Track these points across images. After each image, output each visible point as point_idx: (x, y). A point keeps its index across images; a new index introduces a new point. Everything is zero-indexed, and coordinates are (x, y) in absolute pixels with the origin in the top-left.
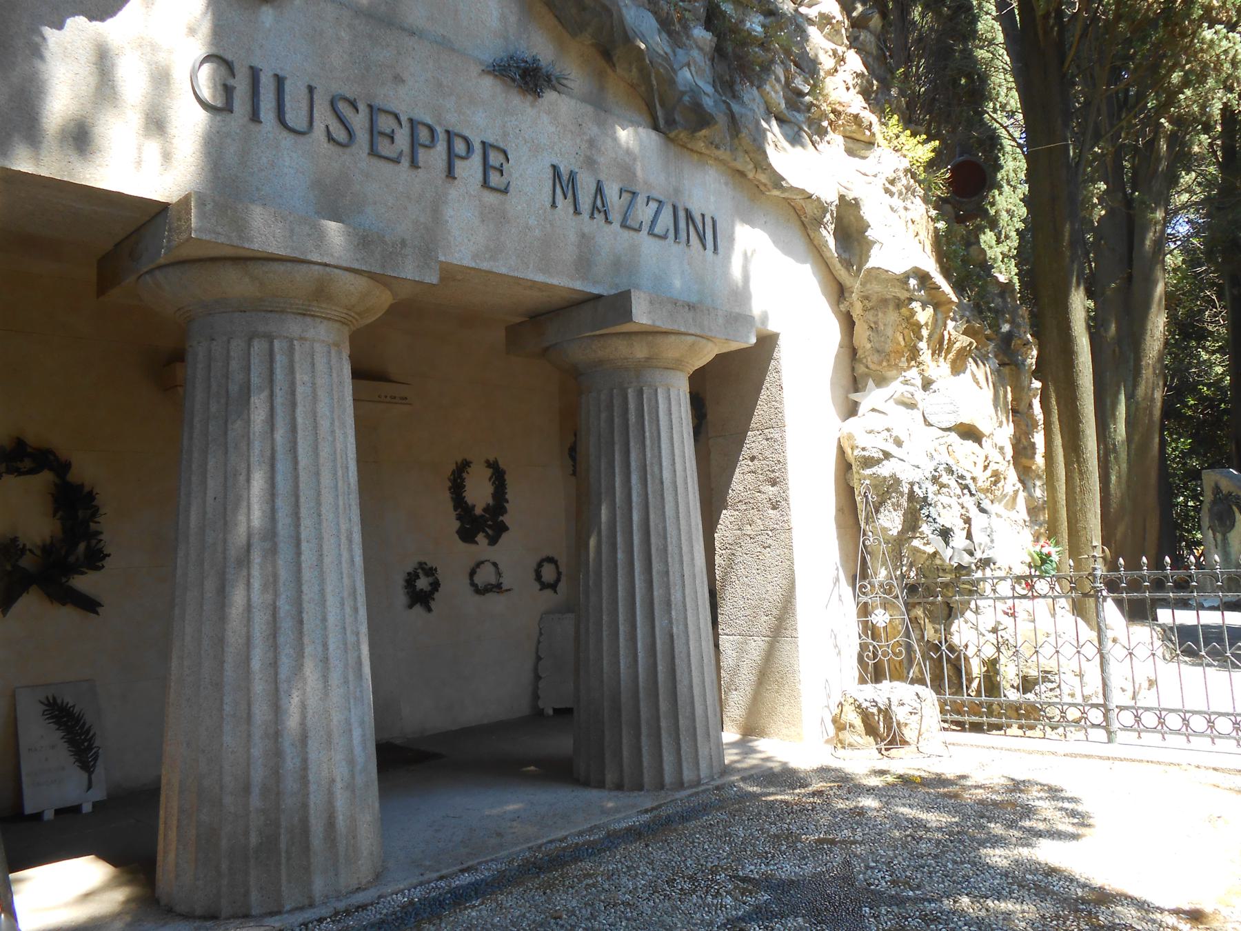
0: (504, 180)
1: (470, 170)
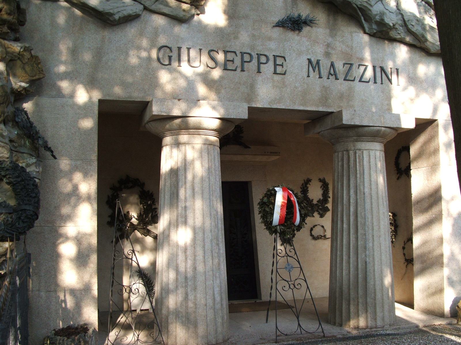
0: (284, 69)
1: (268, 68)
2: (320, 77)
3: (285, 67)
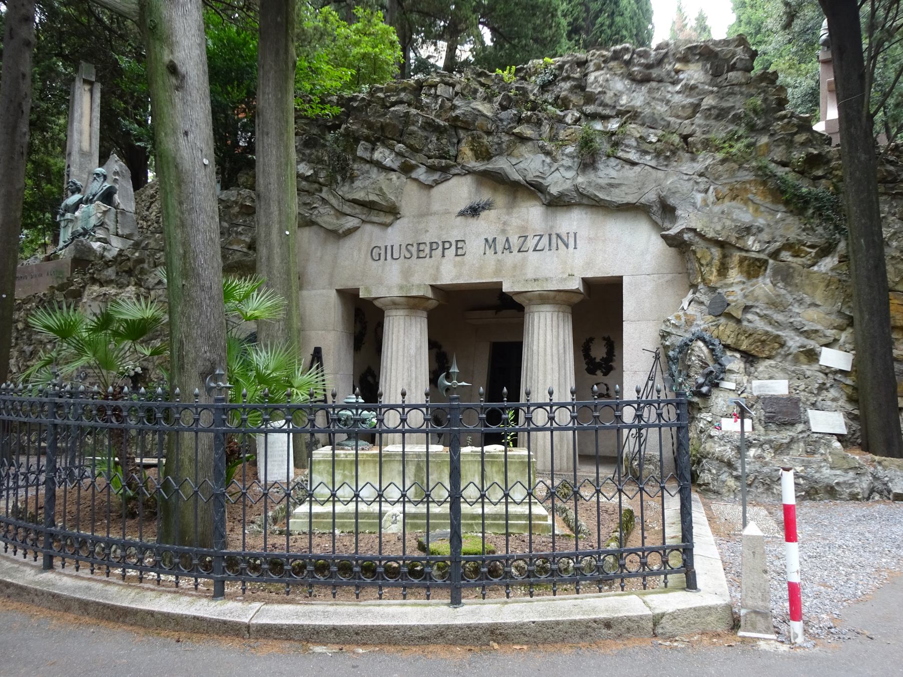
2: (495, 253)
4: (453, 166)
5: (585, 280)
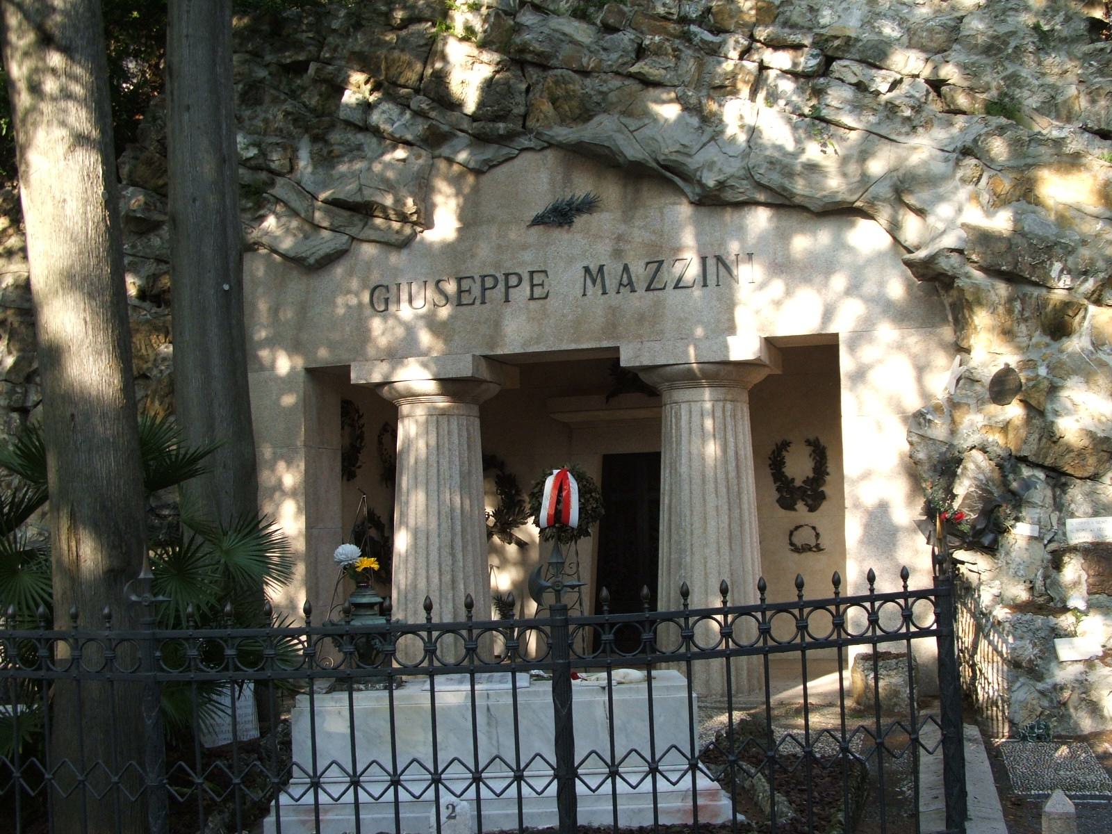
2: (604, 293)
3: (546, 287)
4: (519, 134)
5: (770, 342)
